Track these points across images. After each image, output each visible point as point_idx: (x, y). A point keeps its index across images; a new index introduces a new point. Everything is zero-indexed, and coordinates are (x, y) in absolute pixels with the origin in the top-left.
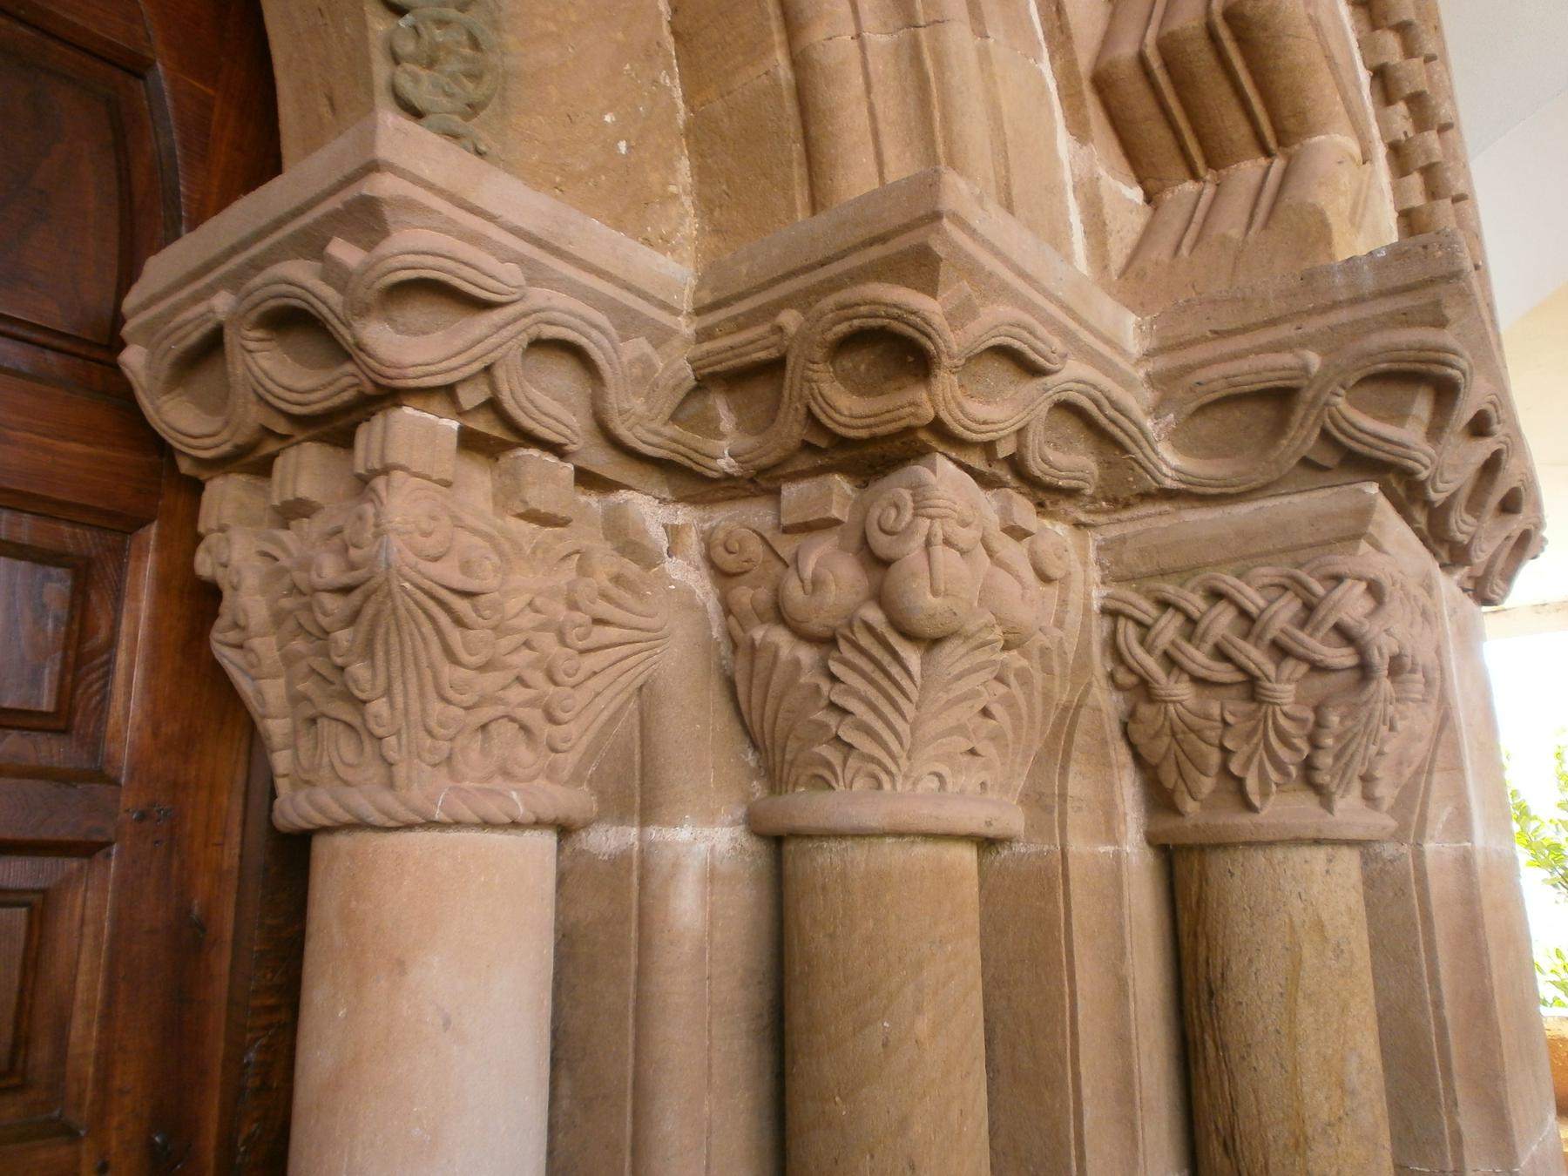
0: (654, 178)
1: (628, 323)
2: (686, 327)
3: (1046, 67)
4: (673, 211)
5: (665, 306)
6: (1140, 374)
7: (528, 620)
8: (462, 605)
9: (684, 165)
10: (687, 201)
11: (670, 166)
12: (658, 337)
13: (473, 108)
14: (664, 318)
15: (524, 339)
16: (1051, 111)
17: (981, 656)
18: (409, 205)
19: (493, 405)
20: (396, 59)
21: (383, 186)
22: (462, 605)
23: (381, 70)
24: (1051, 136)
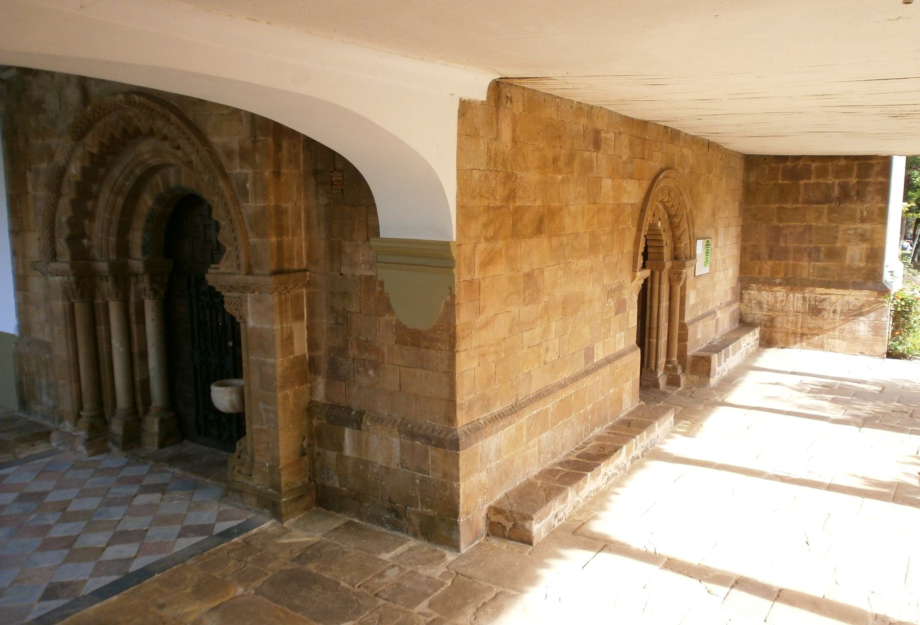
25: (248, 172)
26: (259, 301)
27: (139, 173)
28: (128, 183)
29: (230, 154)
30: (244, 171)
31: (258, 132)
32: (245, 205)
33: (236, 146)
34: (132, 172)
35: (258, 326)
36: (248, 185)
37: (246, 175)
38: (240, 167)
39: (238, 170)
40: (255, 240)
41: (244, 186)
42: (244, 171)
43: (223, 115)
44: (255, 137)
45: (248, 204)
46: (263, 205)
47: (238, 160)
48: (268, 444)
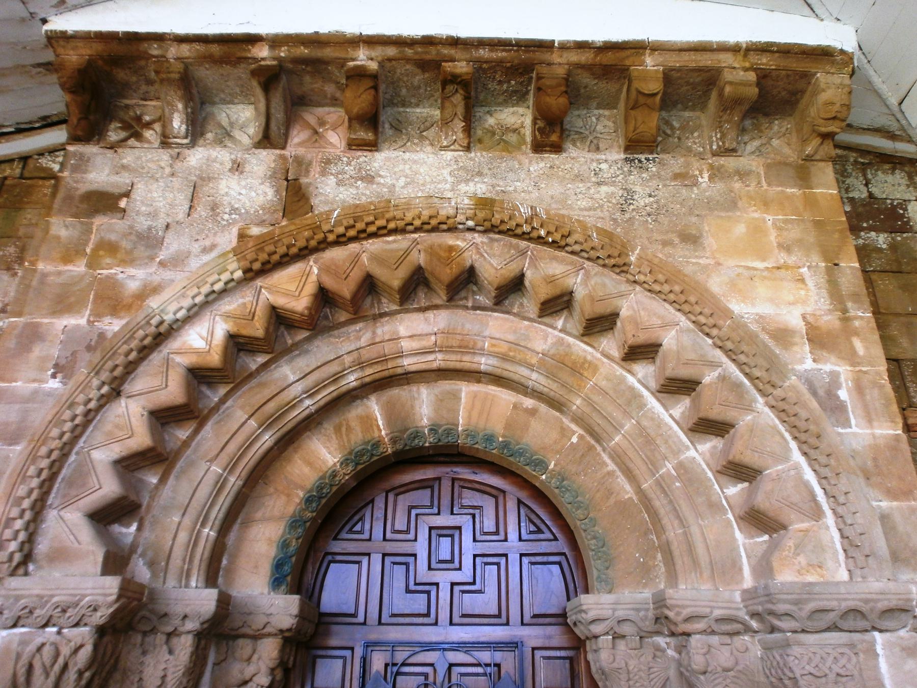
0: (651, 563)
1: (638, 610)
2: (651, 606)
3: (730, 516)
4: (657, 569)
5: (646, 604)
6: (741, 606)
7: (636, 670)
8: (620, 671)
9: (659, 556)
10: (661, 564)
11: (655, 558)
12: (647, 610)
13: (607, 568)
14: (647, 606)
15: (616, 623)
16: (732, 526)
17: (717, 675)
18: (589, 609)
19: (615, 633)
20: (594, 560)
21: (584, 607)
22: (620, 671)
23: (592, 562)
24: (733, 533)
25: (837, 368)
28: (308, 402)
29: (783, 335)
30: (827, 367)
31: (849, 305)
32: (840, 430)
33: (794, 319)
34: (336, 378)
36: (843, 394)
37: (834, 376)
38: (814, 361)
39: (809, 364)
40: (884, 504)
41: (831, 394)
42: (827, 367)
44: (845, 311)
45: (848, 430)
46: (892, 432)
47: (807, 348)
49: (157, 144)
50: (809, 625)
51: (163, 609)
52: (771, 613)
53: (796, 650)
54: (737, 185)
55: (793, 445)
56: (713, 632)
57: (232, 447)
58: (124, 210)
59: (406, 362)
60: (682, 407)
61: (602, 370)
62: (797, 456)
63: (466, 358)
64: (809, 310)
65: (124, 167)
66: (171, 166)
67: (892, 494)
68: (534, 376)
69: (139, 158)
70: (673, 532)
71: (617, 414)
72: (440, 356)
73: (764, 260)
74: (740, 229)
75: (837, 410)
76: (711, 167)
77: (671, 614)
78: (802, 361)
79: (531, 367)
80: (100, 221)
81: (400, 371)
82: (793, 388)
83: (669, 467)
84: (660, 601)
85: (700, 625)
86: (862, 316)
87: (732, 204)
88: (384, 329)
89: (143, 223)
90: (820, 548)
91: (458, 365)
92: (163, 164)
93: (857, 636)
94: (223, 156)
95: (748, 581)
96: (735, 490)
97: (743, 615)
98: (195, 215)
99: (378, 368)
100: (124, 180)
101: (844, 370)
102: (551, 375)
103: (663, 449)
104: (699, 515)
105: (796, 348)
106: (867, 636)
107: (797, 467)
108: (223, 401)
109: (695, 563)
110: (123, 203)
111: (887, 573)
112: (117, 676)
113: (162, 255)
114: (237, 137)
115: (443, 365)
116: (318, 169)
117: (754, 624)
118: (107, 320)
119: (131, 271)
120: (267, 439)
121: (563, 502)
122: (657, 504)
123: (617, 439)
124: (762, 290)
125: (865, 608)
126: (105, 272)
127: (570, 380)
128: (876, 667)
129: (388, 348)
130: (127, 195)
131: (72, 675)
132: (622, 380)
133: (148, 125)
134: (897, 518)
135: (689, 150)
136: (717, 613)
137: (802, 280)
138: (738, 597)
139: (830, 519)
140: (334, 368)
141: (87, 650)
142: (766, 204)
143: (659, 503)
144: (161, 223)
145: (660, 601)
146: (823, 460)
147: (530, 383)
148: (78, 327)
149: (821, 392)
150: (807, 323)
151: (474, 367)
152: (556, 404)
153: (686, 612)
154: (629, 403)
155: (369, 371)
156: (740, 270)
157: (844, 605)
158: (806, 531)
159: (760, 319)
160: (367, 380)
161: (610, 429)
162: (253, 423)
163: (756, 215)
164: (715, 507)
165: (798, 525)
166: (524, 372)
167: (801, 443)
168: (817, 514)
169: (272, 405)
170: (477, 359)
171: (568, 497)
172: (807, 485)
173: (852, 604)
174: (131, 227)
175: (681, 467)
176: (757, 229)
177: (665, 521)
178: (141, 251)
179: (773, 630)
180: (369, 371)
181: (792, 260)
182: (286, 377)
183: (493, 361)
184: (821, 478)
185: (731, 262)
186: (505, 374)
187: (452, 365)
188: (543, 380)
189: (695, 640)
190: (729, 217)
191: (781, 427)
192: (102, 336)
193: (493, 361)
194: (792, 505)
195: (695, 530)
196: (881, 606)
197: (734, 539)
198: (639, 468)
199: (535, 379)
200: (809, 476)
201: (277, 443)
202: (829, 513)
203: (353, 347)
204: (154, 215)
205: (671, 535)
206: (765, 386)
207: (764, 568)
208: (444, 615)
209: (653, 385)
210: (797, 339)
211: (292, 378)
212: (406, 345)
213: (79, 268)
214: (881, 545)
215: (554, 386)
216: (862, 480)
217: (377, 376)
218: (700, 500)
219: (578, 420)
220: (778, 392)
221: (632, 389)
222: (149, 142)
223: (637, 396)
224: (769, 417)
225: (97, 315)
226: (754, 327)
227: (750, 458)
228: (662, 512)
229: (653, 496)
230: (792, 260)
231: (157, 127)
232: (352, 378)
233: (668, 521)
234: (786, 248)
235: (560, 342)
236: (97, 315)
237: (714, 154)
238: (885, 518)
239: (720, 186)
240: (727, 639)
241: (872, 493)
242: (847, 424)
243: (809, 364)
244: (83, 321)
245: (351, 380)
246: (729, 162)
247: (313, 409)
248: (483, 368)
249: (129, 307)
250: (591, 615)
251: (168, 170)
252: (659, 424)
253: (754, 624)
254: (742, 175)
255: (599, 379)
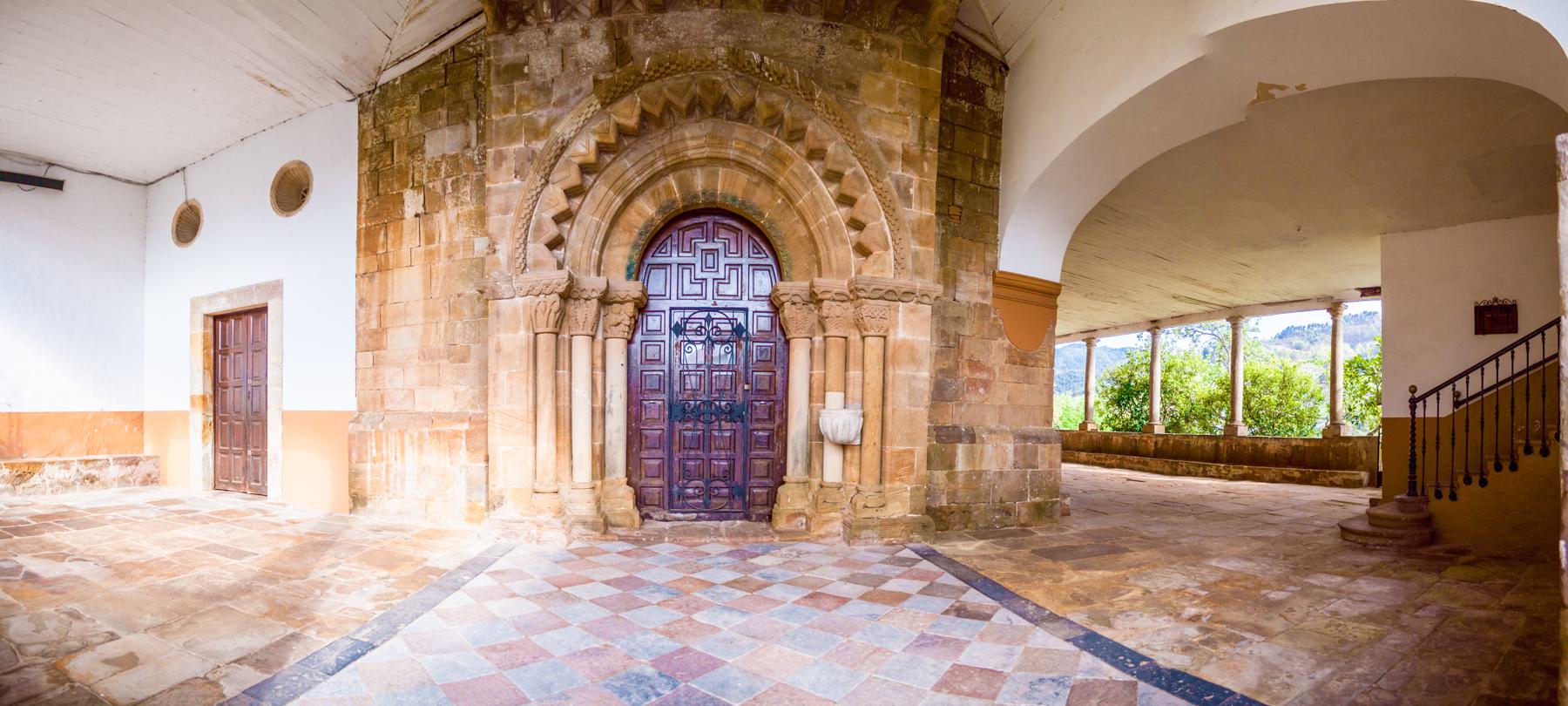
25: (913, 177)
26: (913, 311)
27: (662, 167)
28: (638, 179)
29: (889, 154)
33: (897, 147)
34: (652, 165)
35: (910, 337)
36: (912, 191)
37: (910, 180)
39: (899, 172)
40: (917, 247)
41: (907, 190)
43: (883, 112)
47: (900, 163)
48: (912, 464)
49: (535, 26)
50: (873, 296)
51: (582, 287)
52: (856, 289)
53: (865, 306)
54: (885, 55)
55: (883, 213)
56: (834, 300)
57: (602, 207)
58: (527, 75)
59: (689, 153)
60: (833, 188)
61: (796, 162)
62: (883, 219)
63: (723, 151)
64: (906, 142)
65: (522, 46)
66: (546, 39)
67: (921, 243)
68: (759, 163)
69: (527, 37)
70: (822, 253)
71: (801, 188)
72: (708, 149)
73: (889, 107)
74: (881, 85)
75: (906, 198)
76: (873, 39)
77: (815, 290)
78: (896, 170)
79: (757, 157)
80: (517, 84)
81: (686, 159)
82: (887, 183)
83: (824, 219)
84: (812, 286)
85: (828, 296)
86: (932, 150)
87: (879, 68)
88: (677, 134)
89: (539, 80)
90: (884, 262)
91: (718, 155)
92: (542, 39)
93: (891, 303)
94: (575, 27)
95: (853, 275)
96: (853, 234)
97: (847, 292)
98: (567, 71)
99: (674, 157)
100: (522, 54)
101: (915, 178)
102: (768, 164)
103: (823, 209)
104: (836, 245)
105: (895, 162)
106: (896, 303)
107: (882, 224)
108: (595, 181)
109: (831, 268)
110: (526, 70)
111: (909, 277)
112: (566, 318)
113: (553, 100)
114: (580, 9)
115: (710, 155)
116: (632, 29)
117: (851, 296)
118: (534, 142)
119: (540, 112)
120: (619, 201)
121: (772, 234)
122: (816, 237)
123: (801, 201)
124: (885, 125)
125: (896, 290)
126: (527, 114)
127: (779, 167)
128: (897, 316)
129: (680, 146)
130: (527, 63)
131: (552, 314)
132: (807, 168)
133: (527, 12)
134: (921, 254)
135: (863, 23)
136: (836, 290)
137: (907, 124)
138: (846, 283)
139: (891, 251)
140: (651, 158)
141: (557, 305)
142: (898, 72)
143: (817, 237)
144: (549, 79)
145: (812, 286)
146: (893, 222)
147: (757, 167)
148: (520, 149)
149: (902, 188)
150: (904, 150)
151: (725, 156)
152: (771, 181)
153: (822, 289)
154: (808, 182)
155: (669, 159)
156: (875, 111)
157: (888, 288)
158: (880, 255)
159: (880, 143)
160: (669, 164)
161: (797, 196)
162: (611, 193)
163: (891, 77)
164: (843, 241)
165: (877, 252)
166: (754, 160)
167: (886, 212)
168: (886, 248)
169: (620, 183)
170: (728, 151)
171: (773, 234)
172: (885, 233)
173: (891, 288)
174: (534, 84)
175: (830, 219)
176: (890, 87)
177: (820, 247)
178: (542, 100)
179: (858, 297)
180: (669, 159)
181: (905, 110)
182: (625, 165)
183: (737, 153)
184: (892, 231)
185: (872, 106)
186: (744, 161)
187: (714, 155)
188: (763, 165)
189: (825, 303)
190: (876, 76)
191: (879, 204)
192: (533, 152)
193: (737, 153)
194: (876, 243)
195: (832, 252)
196: (903, 290)
197: (850, 258)
198: (810, 217)
199: (760, 164)
200: (887, 229)
201: (624, 202)
202: (892, 248)
203: (660, 145)
204: (543, 75)
205: (821, 254)
206: (875, 180)
207: (859, 272)
208: (710, 282)
209: (821, 172)
210: (897, 157)
211: (629, 165)
212: (690, 143)
213: (513, 114)
214: (910, 265)
215: (770, 170)
216: (910, 235)
217: (674, 162)
218: (837, 237)
219: (782, 190)
220: (880, 185)
221: (810, 174)
222: (531, 25)
223: (813, 178)
224: (874, 197)
225: (529, 141)
226: (876, 147)
227: (862, 218)
228: (818, 242)
229: (815, 234)
230: (905, 110)
231: (532, 12)
232: (660, 163)
233: (821, 247)
234: (902, 102)
235: (775, 143)
236: (529, 141)
237: (877, 30)
238: (916, 254)
239: (876, 53)
240: (840, 303)
241: (912, 241)
242: (910, 206)
243: (899, 172)
244: (522, 145)
245: (660, 165)
246: (884, 38)
247: (641, 183)
248: (731, 157)
249: (543, 134)
250: (781, 292)
251: (545, 42)
252: (822, 195)
253: (851, 296)
254: (890, 48)
255: (794, 167)
